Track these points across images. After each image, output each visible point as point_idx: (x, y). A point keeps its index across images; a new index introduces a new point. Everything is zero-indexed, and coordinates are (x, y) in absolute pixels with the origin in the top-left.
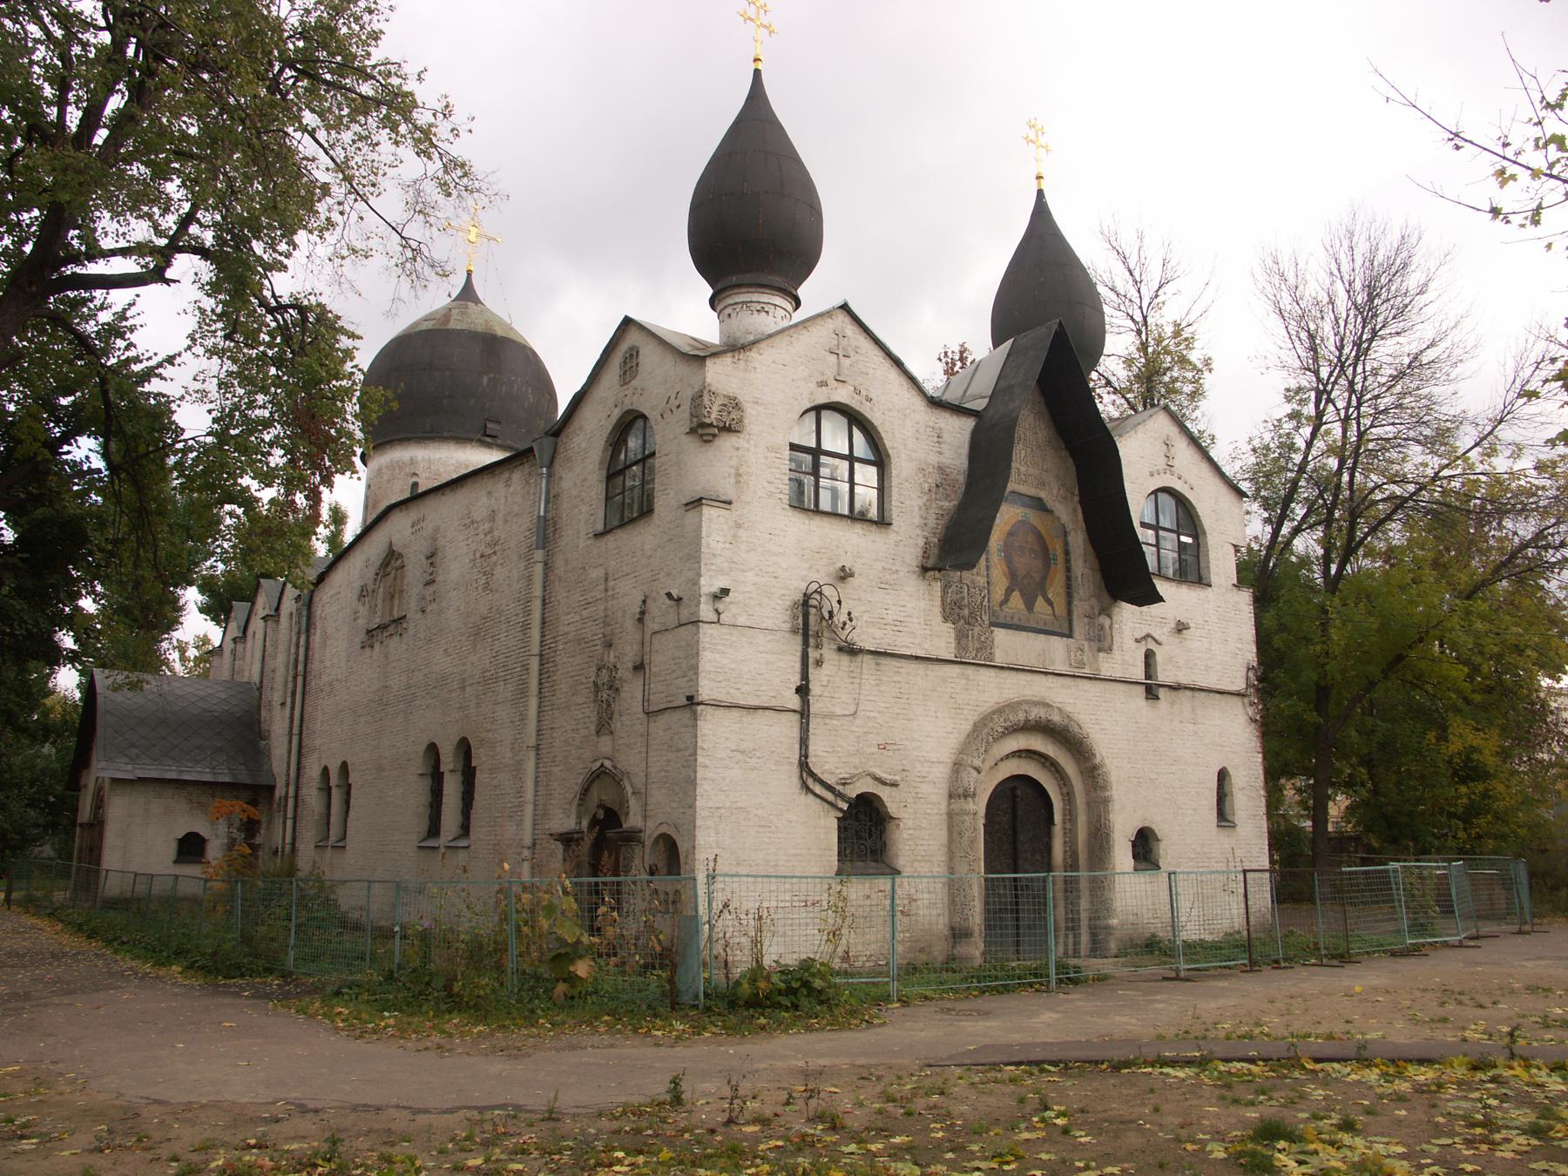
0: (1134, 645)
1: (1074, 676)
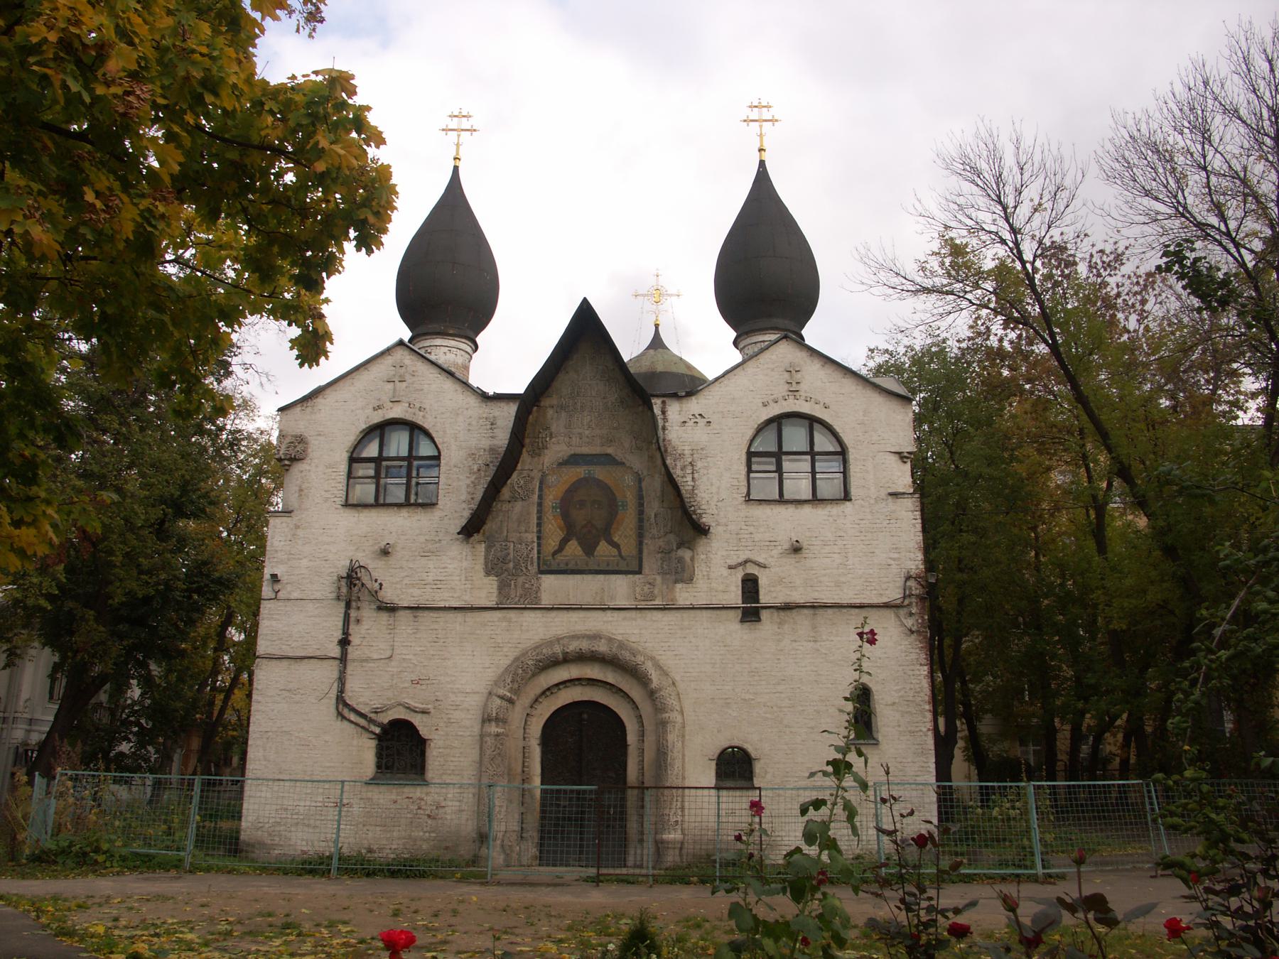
0: (725, 572)
1: (636, 609)
